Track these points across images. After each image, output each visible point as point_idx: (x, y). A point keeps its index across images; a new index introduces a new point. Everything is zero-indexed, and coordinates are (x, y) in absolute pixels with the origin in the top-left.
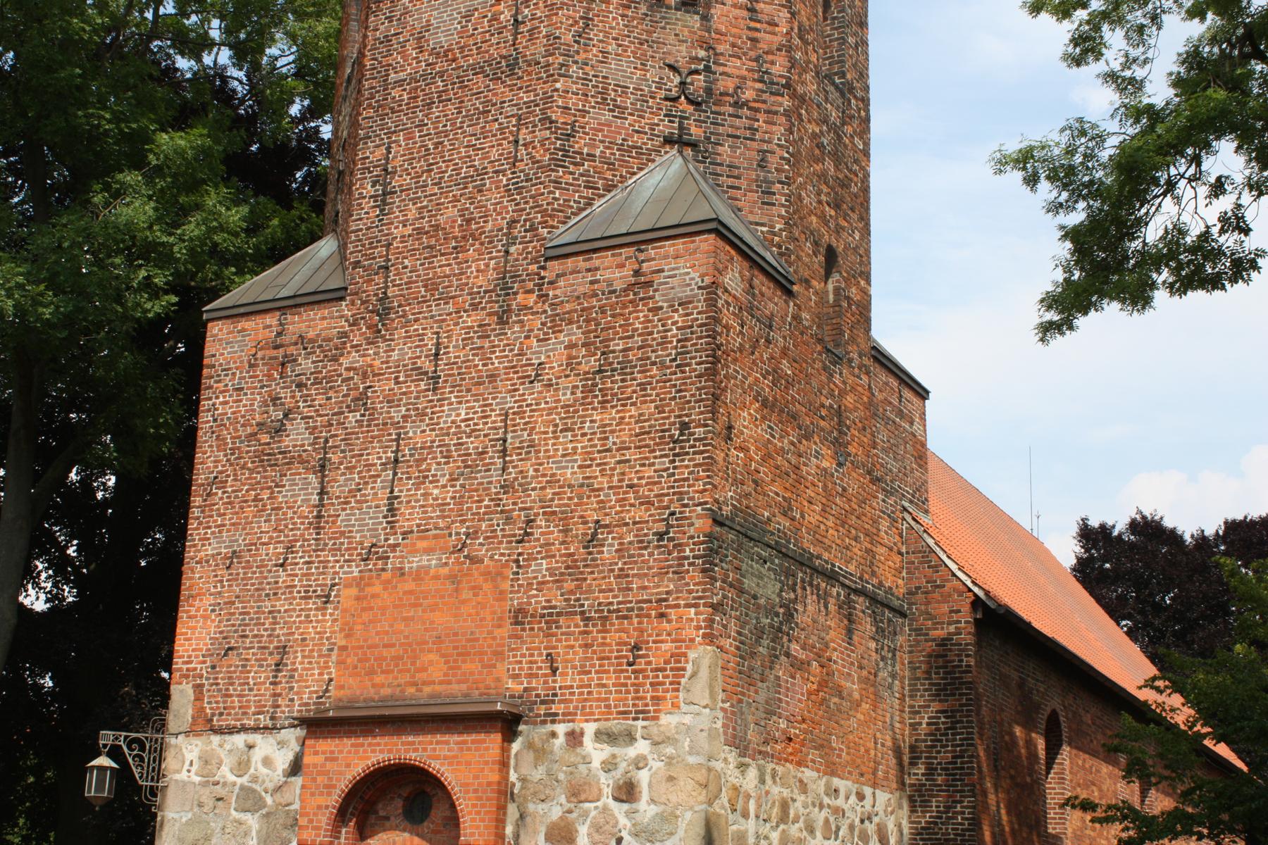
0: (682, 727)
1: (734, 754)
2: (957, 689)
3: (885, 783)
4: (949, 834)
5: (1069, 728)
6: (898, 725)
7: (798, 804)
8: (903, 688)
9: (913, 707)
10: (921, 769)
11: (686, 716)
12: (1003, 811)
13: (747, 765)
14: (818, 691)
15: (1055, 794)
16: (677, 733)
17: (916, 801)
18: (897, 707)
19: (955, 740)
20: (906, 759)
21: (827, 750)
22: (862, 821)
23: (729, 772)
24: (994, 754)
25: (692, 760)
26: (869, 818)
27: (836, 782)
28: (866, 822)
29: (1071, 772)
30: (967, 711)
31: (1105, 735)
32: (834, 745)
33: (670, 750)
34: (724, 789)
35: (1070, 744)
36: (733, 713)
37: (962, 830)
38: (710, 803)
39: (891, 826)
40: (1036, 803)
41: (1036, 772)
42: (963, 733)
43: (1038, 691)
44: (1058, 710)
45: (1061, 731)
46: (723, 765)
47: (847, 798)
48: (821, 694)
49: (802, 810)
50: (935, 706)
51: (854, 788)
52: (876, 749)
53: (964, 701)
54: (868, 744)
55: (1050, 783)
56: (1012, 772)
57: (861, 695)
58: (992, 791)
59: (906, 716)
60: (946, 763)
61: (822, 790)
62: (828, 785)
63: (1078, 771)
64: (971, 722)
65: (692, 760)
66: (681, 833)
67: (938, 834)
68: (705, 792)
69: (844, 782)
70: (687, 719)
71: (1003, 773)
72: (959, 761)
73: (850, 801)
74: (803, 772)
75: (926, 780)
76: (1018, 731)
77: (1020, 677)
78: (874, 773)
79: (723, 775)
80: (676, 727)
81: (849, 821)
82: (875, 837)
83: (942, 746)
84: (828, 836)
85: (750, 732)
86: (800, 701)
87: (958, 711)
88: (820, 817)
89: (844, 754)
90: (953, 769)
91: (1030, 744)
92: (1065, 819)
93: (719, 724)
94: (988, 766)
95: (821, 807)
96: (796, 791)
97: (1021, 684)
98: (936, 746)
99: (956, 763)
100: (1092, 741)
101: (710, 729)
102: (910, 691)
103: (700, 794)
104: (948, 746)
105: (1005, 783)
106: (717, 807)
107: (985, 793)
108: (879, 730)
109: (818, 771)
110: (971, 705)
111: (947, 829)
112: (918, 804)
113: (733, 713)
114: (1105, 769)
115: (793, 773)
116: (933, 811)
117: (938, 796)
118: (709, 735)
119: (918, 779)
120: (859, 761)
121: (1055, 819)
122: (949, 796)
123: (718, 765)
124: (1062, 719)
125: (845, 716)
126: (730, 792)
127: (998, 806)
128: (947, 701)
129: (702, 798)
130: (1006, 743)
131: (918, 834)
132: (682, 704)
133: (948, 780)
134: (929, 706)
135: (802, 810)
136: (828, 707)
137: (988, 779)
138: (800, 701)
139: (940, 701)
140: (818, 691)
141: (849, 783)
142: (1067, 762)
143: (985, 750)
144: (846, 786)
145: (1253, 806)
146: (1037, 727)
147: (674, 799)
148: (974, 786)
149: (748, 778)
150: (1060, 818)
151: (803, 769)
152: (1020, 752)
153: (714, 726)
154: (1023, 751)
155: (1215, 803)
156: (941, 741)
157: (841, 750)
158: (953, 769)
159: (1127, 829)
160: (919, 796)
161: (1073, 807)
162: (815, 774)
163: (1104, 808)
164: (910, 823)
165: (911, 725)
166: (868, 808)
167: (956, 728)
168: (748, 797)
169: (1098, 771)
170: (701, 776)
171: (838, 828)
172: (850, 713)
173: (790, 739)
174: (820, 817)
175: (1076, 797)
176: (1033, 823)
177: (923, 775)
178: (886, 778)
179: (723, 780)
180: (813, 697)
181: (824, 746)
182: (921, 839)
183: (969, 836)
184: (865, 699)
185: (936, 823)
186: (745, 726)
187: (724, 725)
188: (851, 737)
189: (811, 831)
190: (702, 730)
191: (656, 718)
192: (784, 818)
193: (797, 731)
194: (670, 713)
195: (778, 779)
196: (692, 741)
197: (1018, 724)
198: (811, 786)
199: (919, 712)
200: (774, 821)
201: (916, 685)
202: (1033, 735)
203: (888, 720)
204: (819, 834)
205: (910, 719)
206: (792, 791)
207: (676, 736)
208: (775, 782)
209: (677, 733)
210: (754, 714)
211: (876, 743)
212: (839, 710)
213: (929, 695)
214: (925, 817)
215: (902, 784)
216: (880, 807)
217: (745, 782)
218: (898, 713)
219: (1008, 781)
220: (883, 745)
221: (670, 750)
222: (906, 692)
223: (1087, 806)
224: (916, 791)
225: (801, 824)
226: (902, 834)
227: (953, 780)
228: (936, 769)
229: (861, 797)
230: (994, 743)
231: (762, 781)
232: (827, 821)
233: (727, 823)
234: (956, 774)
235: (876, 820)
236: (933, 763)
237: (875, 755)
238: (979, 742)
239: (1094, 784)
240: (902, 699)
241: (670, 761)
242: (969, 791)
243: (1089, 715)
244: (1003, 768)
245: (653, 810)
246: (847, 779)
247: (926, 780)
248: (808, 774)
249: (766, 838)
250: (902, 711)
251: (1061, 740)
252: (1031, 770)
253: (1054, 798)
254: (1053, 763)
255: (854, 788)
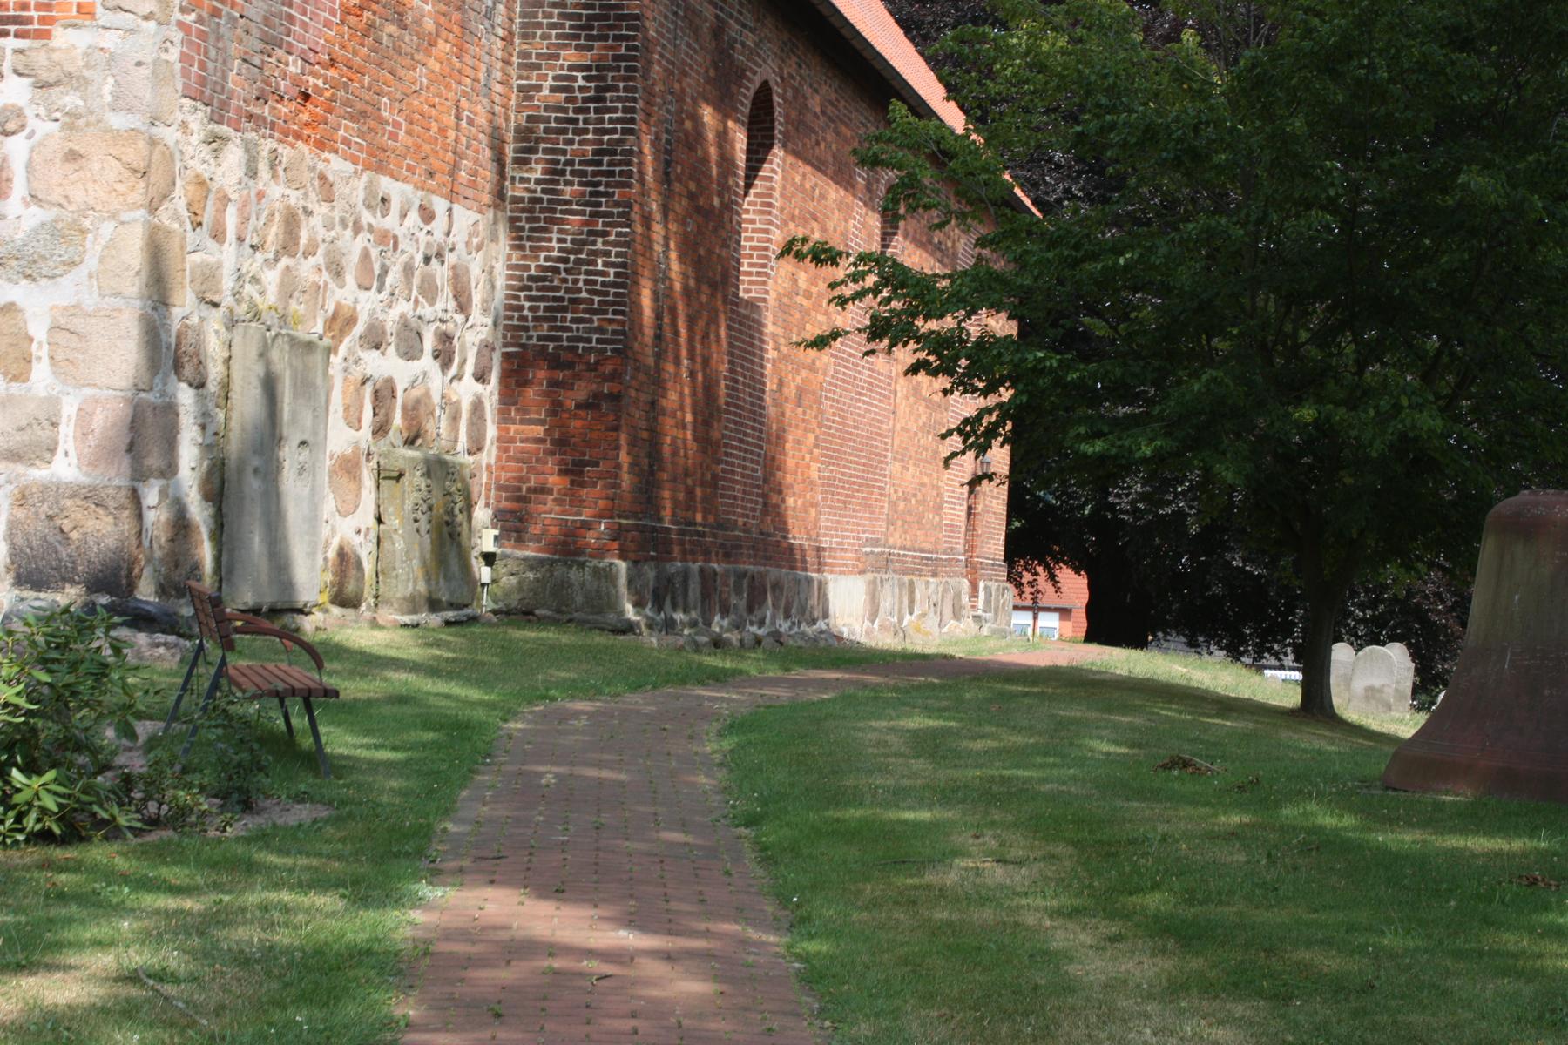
0: (98, 55)
1: (200, 115)
2: (611, 27)
3: (470, 193)
4: (579, 291)
5: (787, 116)
6: (498, 88)
7: (316, 221)
8: (511, 20)
9: (526, 55)
10: (537, 171)
11: (108, 34)
12: (673, 255)
13: (225, 140)
14: (361, 8)
15: (754, 231)
16: (87, 66)
17: (522, 229)
18: (499, 54)
19: (602, 121)
20: (510, 151)
21: (371, 123)
22: (427, 260)
23: (190, 151)
24: (667, 152)
25: (118, 121)
26: (439, 255)
27: (386, 184)
28: (434, 261)
29: (782, 195)
30: (627, 69)
31: (838, 133)
32: (385, 114)
33: (72, 100)
34: (179, 182)
35: (784, 146)
36: (202, 35)
37: (604, 284)
38: (152, 209)
39: (475, 271)
40: (725, 245)
41: (729, 189)
42: (615, 110)
43: (743, 44)
44: (772, 84)
45: (772, 121)
46: (179, 135)
47: (404, 216)
48: (366, 14)
49: (322, 233)
50: (570, 56)
51: (417, 197)
52: (458, 128)
53: (623, 51)
54: (445, 118)
55: (747, 211)
56: (692, 186)
57: (438, 25)
58: (658, 216)
59: (514, 71)
60: (581, 163)
61: (359, 196)
62: (370, 188)
63: (793, 195)
64: (633, 89)
65: (118, 121)
66: (91, 263)
67: (557, 289)
68: (142, 184)
69: (399, 184)
70: (110, 40)
71: (677, 187)
72: (606, 159)
73: (409, 222)
74: (327, 161)
75: (543, 191)
76: (707, 114)
77: (717, 17)
78: (452, 174)
79: (177, 156)
80: (86, 54)
81: (404, 258)
82: (448, 291)
83: (577, 132)
84: (366, 284)
85: (232, 76)
86: (327, 24)
87: (610, 69)
88: (353, 247)
89: (402, 133)
90: (594, 174)
91: (723, 137)
92: (767, 275)
93: (174, 54)
94: (655, 171)
95: (357, 228)
96: (313, 195)
97: (718, 31)
98: (565, 131)
99: (600, 163)
100: (818, 143)
101: (156, 62)
102: (524, 26)
103: (133, 189)
104: (586, 131)
105: (680, 205)
106: (164, 217)
107: (647, 220)
108: (465, 94)
109: (355, 161)
110: (634, 59)
111: (576, 281)
112: (525, 234)
113: (202, 35)
114: (834, 193)
115: (308, 162)
116: (550, 249)
117: (562, 221)
118: (153, 72)
119: (528, 190)
120: (427, 148)
121: (750, 274)
122: (586, 223)
123: (170, 135)
124: (776, 99)
125: (407, 61)
126: (191, 188)
127: (667, 245)
128: (591, 48)
129: (138, 196)
130: (686, 134)
131: (522, 289)
132: (99, 10)
133: (583, 194)
134: (557, 57)
135: (322, 233)
136: (378, 41)
137: (654, 195)
138: (327, 24)
139: (578, 47)
140: (361, 8)
141: (409, 188)
142: (778, 177)
143: (653, 144)
144: (403, 193)
145: (1122, 261)
146: (736, 110)
147: (78, 195)
148: (630, 206)
149: (225, 164)
150: (758, 274)
151: (326, 155)
152: (706, 153)
153: (164, 56)
154: (713, 151)
155: (1050, 255)
156: (574, 121)
157: (397, 125)
158: (594, 174)
159: (888, 301)
160: (528, 220)
161: (800, 256)
162: (349, 167)
163: (852, 259)
164: (510, 267)
165: (521, 89)
166: (439, 235)
167: (603, 100)
168: (225, 200)
169: (823, 197)
170: (136, 154)
171: (385, 271)
172: (417, 57)
173: (306, 97)
174: (353, 247)
175: (805, 240)
176: (718, 278)
177: (538, 182)
178: (473, 185)
179: (178, 165)
180: (352, 19)
181: (365, 115)
182: (529, 298)
183: (615, 294)
184: (444, 33)
185: (556, 270)
186: (224, 63)
187: (184, 58)
188: (416, 102)
189: (338, 273)
190: (139, 64)
191: (44, 35)
192: (289, 245)
193: (320, 83)
194: (74, 26)
195: (280, 170)
196: (118, 84)
197: (707, 101)
198: (340, 189)
199: (538, 67)
200: (271, 249)
201: (535, 15)
202: (730, 124)
203: (482, 76)
204: (350, 279)
205: (520, 77)
206: (306, 195)
207: (86, 73)
208: (274, 176)
209: (87, 66)
210: (240, 42)
211: (458, 117)
212: (398, 51)
213: (558, 36)
214: (537, 258)
215: (500, 194)
216: (459, 237)
217: (219, 171)
218: (499, 65)
219: (685, 202)
220: (471, 122)
221: (72, 100)
222: (516, 29)
223: (824, 256)
224: (523, 210)
225: (319, 259)
226: (493, 287)
227: (592, 194)
228: (563, 173)
229: (427, 215)
230: (667, 131)
231: (252, 173)
232: (366, 255)
233: (182, 247)
234: (598, 184)
235: (451, 259)
236: (558, 162)
237: (456, 141)
238: (644, 127)
239: (815, 219)
240: (508, 40)
241: (71, 120)
242: (620, 215)
243: (817, 98)
244: (679, 180)
245: (35, 216)
246: (405, 180)
247: (543, 191)
248: (336, 165)
249: (255, 280)
250: (507, 62)
251: (772, 137)
252: (724, 188)
253: (751, 239)
254: (755, 177)
255: (417, 197)
